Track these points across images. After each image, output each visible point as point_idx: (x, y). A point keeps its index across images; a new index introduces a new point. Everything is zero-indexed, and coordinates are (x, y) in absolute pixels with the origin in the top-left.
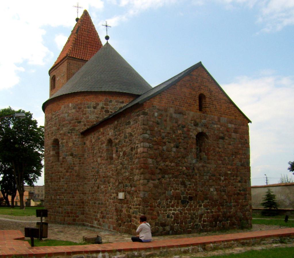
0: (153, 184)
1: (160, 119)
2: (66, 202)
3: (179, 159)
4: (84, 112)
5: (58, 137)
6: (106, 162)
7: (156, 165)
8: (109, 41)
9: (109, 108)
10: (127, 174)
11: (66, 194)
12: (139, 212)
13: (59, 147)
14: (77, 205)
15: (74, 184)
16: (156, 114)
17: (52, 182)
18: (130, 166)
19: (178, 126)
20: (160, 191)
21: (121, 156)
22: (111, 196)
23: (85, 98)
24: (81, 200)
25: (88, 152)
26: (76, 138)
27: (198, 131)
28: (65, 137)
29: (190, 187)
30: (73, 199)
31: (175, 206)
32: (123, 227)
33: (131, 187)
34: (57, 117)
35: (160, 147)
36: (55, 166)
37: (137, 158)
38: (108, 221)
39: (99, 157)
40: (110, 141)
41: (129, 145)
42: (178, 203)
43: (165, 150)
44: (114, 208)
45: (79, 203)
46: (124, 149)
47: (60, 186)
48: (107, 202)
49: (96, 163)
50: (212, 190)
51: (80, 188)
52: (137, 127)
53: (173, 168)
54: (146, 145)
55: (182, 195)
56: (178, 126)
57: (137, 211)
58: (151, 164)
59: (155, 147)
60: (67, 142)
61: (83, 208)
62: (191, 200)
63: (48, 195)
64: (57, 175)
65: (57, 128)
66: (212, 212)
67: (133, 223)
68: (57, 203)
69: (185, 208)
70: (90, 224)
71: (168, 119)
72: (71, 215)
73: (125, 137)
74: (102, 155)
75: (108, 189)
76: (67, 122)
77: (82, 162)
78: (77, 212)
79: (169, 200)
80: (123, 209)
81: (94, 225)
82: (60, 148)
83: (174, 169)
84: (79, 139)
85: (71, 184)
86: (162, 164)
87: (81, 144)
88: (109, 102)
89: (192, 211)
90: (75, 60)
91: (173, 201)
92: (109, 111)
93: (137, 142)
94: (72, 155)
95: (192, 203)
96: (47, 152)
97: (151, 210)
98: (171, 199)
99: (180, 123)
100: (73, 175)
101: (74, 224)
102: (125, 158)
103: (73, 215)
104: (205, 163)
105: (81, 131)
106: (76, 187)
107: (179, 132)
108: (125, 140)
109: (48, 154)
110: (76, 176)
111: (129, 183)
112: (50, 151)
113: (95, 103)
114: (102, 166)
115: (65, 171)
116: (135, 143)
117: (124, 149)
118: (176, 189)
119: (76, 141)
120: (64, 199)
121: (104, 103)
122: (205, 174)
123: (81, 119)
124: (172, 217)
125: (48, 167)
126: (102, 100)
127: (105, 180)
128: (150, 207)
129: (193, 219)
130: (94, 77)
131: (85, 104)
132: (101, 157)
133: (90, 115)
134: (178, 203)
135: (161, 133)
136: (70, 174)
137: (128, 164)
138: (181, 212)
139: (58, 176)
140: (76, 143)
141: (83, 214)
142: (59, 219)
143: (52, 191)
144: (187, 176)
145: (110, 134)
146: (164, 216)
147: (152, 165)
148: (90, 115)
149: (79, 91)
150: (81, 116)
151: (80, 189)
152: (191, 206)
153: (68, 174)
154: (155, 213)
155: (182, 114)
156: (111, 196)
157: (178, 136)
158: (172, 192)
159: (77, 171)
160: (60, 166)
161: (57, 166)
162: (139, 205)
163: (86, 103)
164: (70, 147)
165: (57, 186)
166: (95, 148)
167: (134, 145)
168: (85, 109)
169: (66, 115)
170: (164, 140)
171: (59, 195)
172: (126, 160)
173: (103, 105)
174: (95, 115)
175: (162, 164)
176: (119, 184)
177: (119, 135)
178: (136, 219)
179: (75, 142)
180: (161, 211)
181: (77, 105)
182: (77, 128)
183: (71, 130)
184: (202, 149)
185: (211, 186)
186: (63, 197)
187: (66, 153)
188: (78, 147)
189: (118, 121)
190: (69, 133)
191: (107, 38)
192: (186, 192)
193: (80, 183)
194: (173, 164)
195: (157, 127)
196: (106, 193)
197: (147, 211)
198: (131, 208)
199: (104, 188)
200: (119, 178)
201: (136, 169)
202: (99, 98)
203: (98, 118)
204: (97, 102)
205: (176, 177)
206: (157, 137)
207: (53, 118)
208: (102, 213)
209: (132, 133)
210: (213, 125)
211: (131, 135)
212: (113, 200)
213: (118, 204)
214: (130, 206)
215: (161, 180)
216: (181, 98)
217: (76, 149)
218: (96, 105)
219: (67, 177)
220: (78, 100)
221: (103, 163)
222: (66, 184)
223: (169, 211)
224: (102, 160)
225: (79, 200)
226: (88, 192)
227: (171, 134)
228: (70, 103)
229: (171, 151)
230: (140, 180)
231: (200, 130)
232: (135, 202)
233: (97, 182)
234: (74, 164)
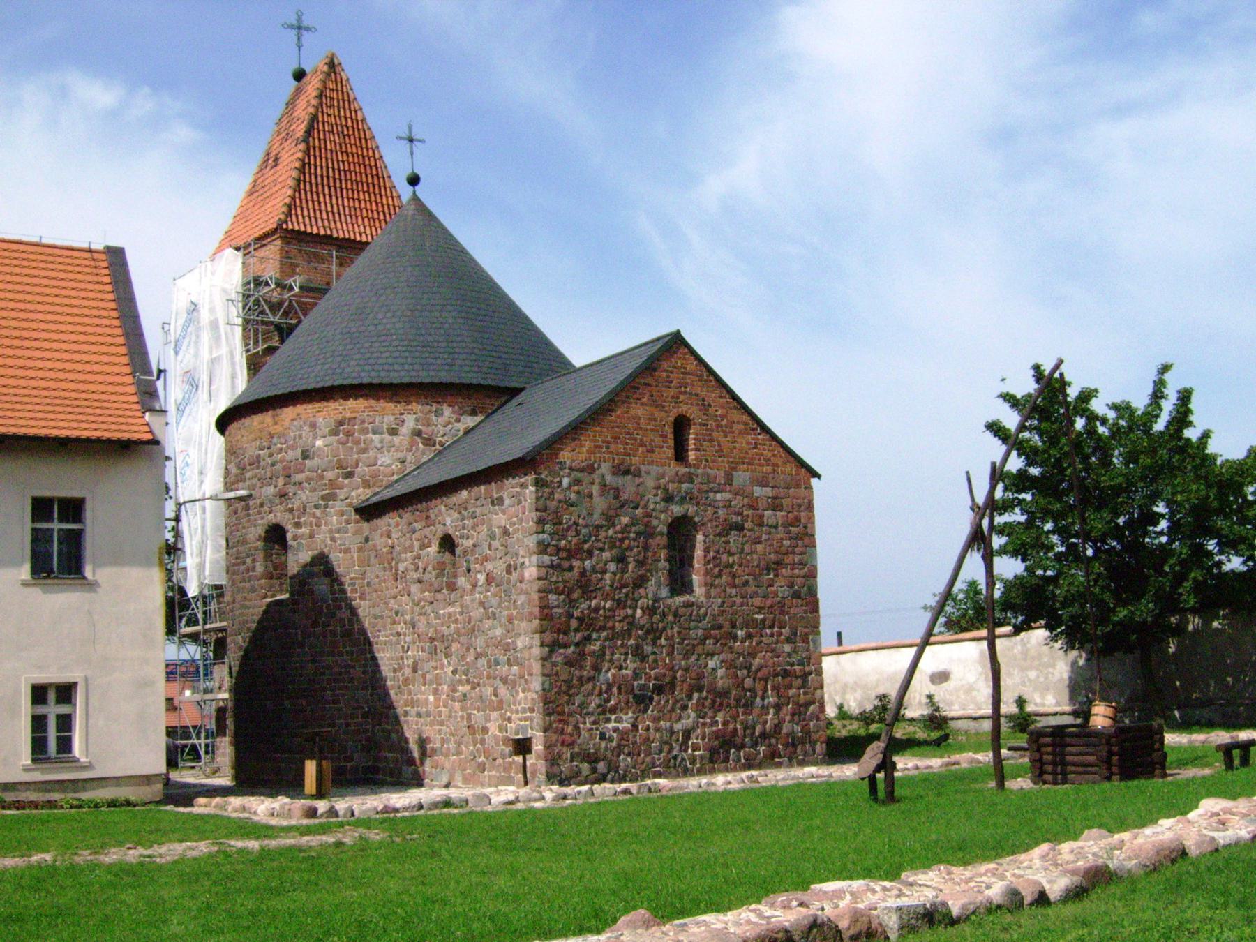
8: (419, 189)
12: (532, 729)
18: (505, 613)
29: (655, 661)
33: (510, 665)
35: (576, 563)
37: (522, 592)
46: (489, 566)
48: (443, 709)
71: (595, 489)
73: (492, 536)
93: (521, 552)
96: (244, 563)
99: (624, 497)
109: (248, 570)
111: (505, 655)
112: (254, 560)
116: (517, 554)
122: (693, 624)
131: (363, 422)
132: (420, 581)
133: (379, 456)
137: (499, 605)
146: (592, 737)
147: (560, 610)
154: (570, 729)
162: (532, 710)
172: (495, 595)
177: (473, 528)
181: (341, 423)
189: (470, 492)
190: (316, 507)
191: (414, 180)
195: (571, 514)
198: (509, 720)
201: (522, 620)
210: (711, 495)
214: (509, 714)
222: (314, 661)
229: (604, 572)
231: (677, 510)
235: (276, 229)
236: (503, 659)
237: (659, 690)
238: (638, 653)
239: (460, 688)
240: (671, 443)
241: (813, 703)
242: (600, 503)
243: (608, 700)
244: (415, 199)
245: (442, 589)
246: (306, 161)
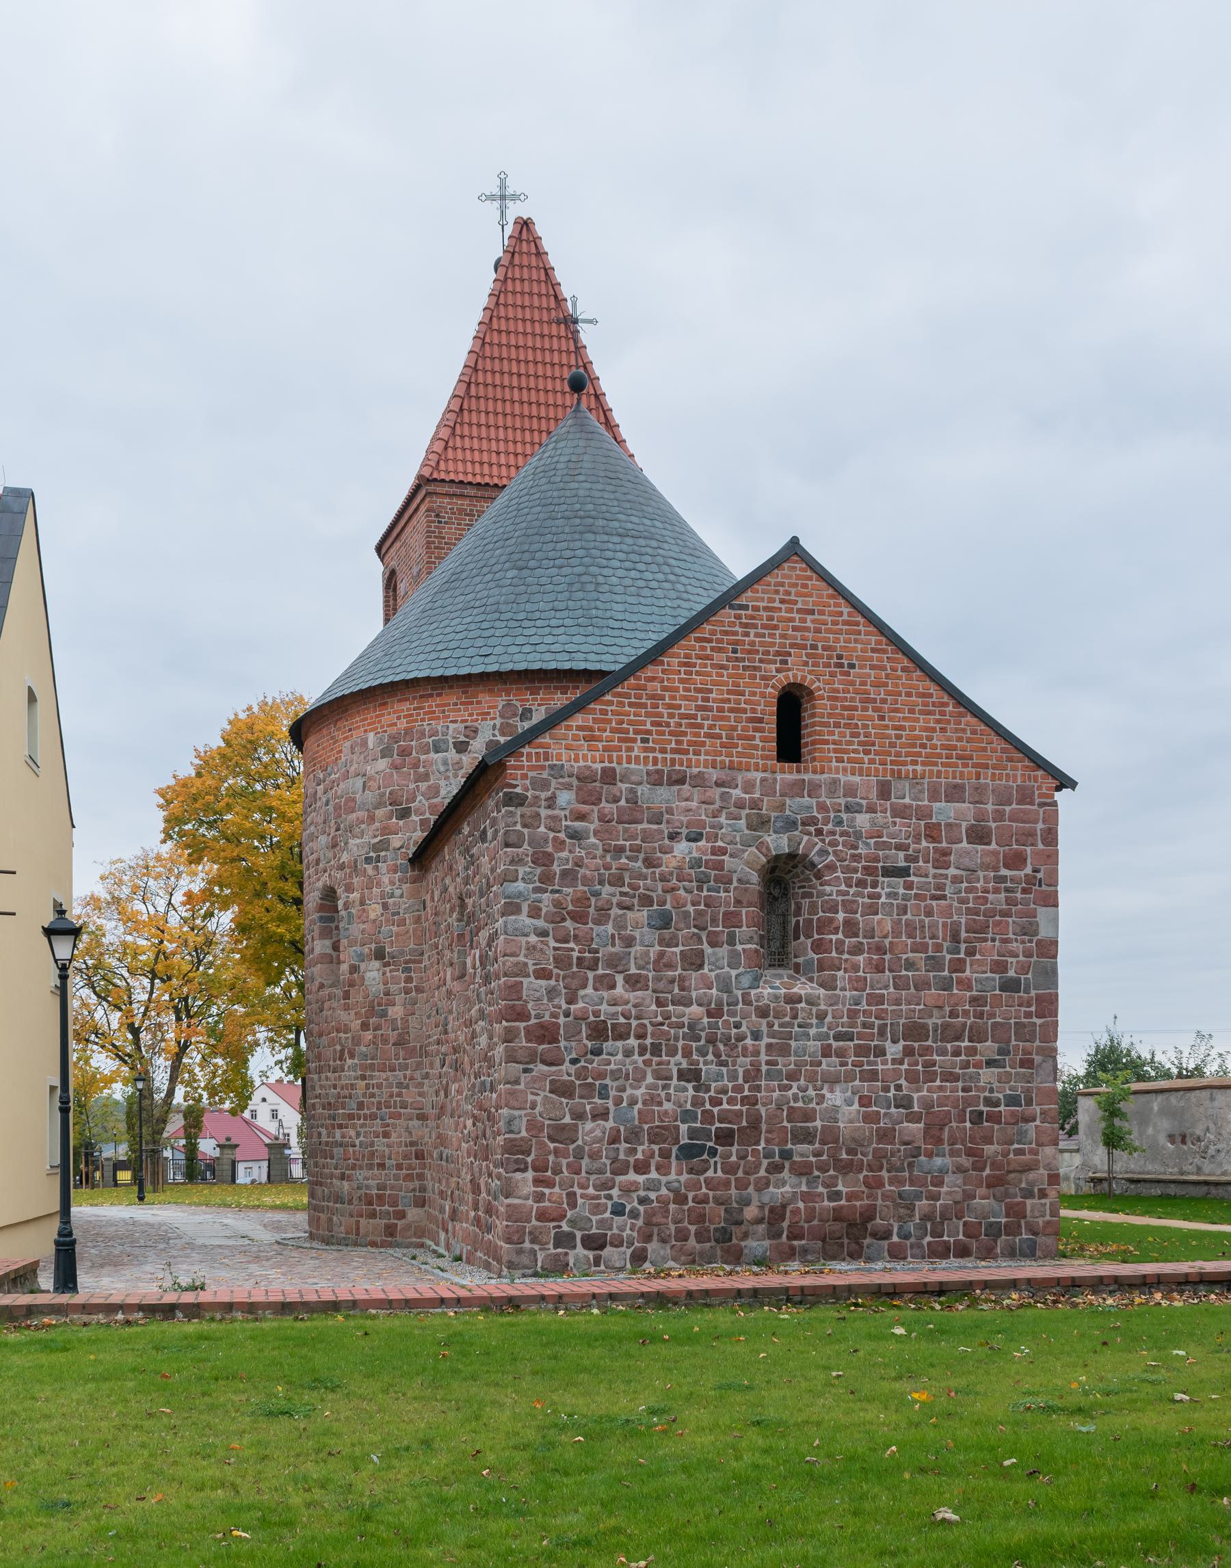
2: (363, 1156)
4: (421, 770)
11: (362, 1121)
15: (386, 1079)
17: (320, 1071)
23: (423, 708)
24: (412, 1144)
26: (392, 883)
28: (355, 880)
31: (653, 1168)
36: (327, 1005)
45: (406, 1157)
51: (410, 1096)
55: (683, 1122)
60: (362, 903)
61: (421, 1177)
66: (835, 1196)
76: (362, 814)
78: (402, 1194)
84: (405, 886)
85: (379, 1077)
90: (462, 496)
94: (379, 955)
95: (734, 1158)
100: (385, 1041)
101: (391, 1245)
103: (386, 1207)
106: (395, 1090)
115: (359, 1022)
119: (392, 896)
120: (357, 1143)
121: (498, 726)
123: (408, 801)
126: (488, 713)
128: (535, 1169)
131: (423, 734)
133: (442, 783)
134: (665, 1154)
136: (375, 1037)
138: (676, 1192)
139: (338, 1048)
140: (394, 904)
141: (421, 1203)
142: (342, 1229)
146: (597, 1209)
148: (442, 783)
149: (397, 678)
150: (412, 786)
151: (410, 1100)
152: (730, 1169)
153: (368, 1035)
159: (399, 1022)
161: (335, 1005)
164: (375, 921)
165: (335, 1087)
168: (423, 757)
169: (359, 782)
171: (340, 1126)
173: (494, 735)
179: (391, 901)
180: (583, 1186)
181: (395, 738)
182: (396, 841)
183: (375, 848)
185: (838, 1081)
187: (358, 949)
188: (402, 923)
190: (368, 860)
193: (408, 1073)
202: (478, 703)
204: (469, 724)
217: (395, 929)
218: (466, 736)
219: (364, 1049)
220: (399, 718)
222: (363, 1078)
225: (406, 1146)
228: (371, 730)
231: (779, 843)
234: (387, 994)
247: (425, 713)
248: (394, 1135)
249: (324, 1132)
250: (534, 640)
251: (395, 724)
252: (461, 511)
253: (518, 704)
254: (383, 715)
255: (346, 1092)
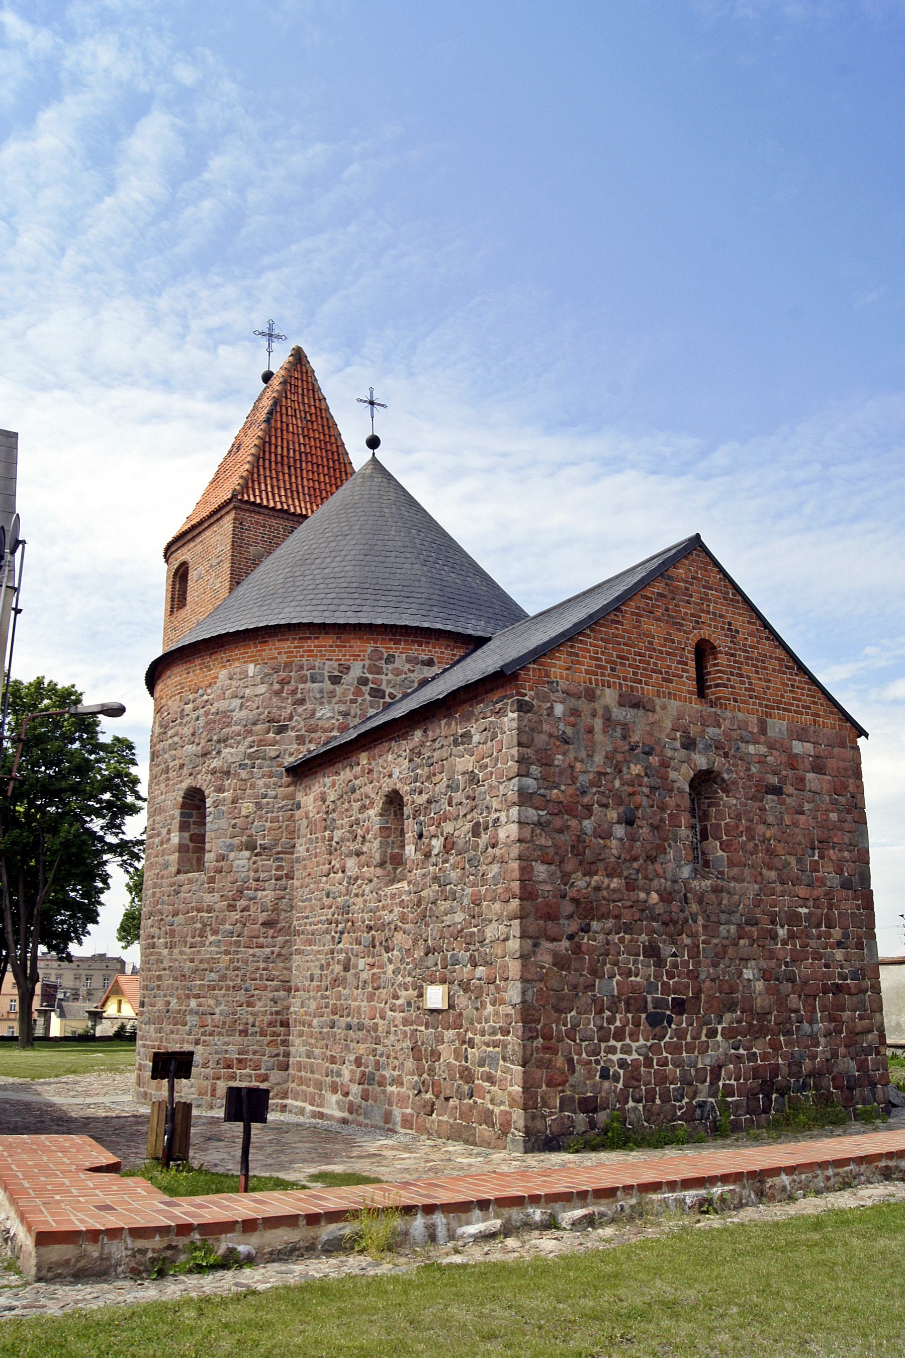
0: (556, 955)
1: (574, 725)
2: (224, 1023)
3: (636, 865)
5: (203, 781)
6: (379, 871)
7: (563, 887)
9: (384, 682)
10: (459, 917)
11: (223, 992)
13: (204, 816)
14: (263, 1034)
16: (559, 709)
17: (171, 946)
18: (469, 890)
19: (632, 749)
20: (572, 978)
21: (435, 852)
22: (396, 997)
23: (303, 647)
25: (309, 836)
27: (695, 764)
29: (675, 965)
30: (250, 1009)
32: (440, 1118)
33: (475, 966)
34: (202, 711)
35: (573, 823)
36: (186, 887)
38: (384, 1092)
39: (350, 855)
40: (394, 801)
41: (465, 815)
42: (637, 1024)
43: (589, 831)
44: (408, 1044)
45: (270, 1024)
46: (448, 827)
47: (201, 961)
48: (381, 1022)
49: (340, 874)
50: (748, 974)
52: (495, 754)
53: (616, 896)
54: (527, 817)
56: (632, 749)
57: (498, 1052)
58: (544, 882)
59: (558, 822)
60: (234, 802)
61: (285, 1043)
62: (681, 1013)
63: (155, 997)
64: (193, 920)
65: (199, 748)
67: (479, 1101)
68: (187, 1028)
69: (662, 1044)
70: (309, 1108)
71: (598, 724)
72: (238, 1072)
74: (365, 849)
75: (384, 973)
76: (236, 728)
77: (285, 872)
78: (266, 1058)
79: (608, 1013)
80: (440, 1048)
81: (325, 1111)
82: (208, 819)
83: (619, 901)
86: (581, 882)
87: (283, 806)
88: (383, 661)
89: (684, 1054)
91: (618, 1016)
92: (384, 692)
93: (495, 805)
94: (250, 846)
97: (546, 1049)
98: (614, 1008)
99: (635, 738)
102: (452, 860)
104: (723, 879)
105: (289, 761)
106: (262, 965)
107: (636, 769)
108: (451, 798)
109: (162, 843)
110: (264, 924)
113: (336, 664)
114: (364, 886)
117: (448, 827)
118: (630, 971)
119: (265, 796)
120: (217, 1011)
124: (616, 1079)
125: (158, 890)
126: (359, 656)
127: (374, 938)
129: (690, 1084)
130: (332, 575)
131: (301, 667)
132: (358, 854)
134: (637, 1024)
135: (575, 774)
137: (461, 880)
140: (268, 803)
143: (170, 981)
144: (665, 924)
145: (396, 772)
146: (590, 1074)
147: (549, 888)
149: (282, 622)
153: (236, 916)
154: (560, 1061)
155: (644, 708)
156: (396, 997)
157: (631, 784)
158: (614, 983)
160: (206, 886)
163: (305, 663)
164: (247, 817)
165: (192, 961)
166: (339, 822)
167: (484, 815)
168: (301, 686)
170: (586, 800)
171: (198, 996)
172: (454, 867)
174: (336, 706)
175: (581, 883)
176: (427, 954)
178: (493, 1083)
182: (272, 751)
183: (250, 756)
184: (709, 827)
186: (211, 1002)
187: (229, 841)
192: (663, 984)
194: (615, 883)
195: (564, 754)
196: (378, 988)
197: (535, 1055)
199: (367, 967)
200: (427, 930)
203: (346, 714)
204: (342, 662)
205: (628, 929)
206: (563, 787)
207: (188, 715)
208: (358, 1062)
209: (476, 771)
211: (473, 779)
212: (402, 1014)
213: (422, 1028)
214: (470, 1035)
215: (576, 939)
216: (640, 655)
217: (268, 824)
218: (341, 672)
220: (280, 653)
221: (367, 875)
222: (227, 953)
223: (607, 1052)
224: (363, 867)
225: (272, 1014)
226: (307, 983)
227: (608, 777)
228: (251, 662)
230: (507, 939)
232: (487, 1021)
233: (341, 946)
235: (231, 500)
236: (464, 956)
237: (680, 1006)
238: (652, 952)
239: (403, 993)
240: (693, 673)
241: (870, 1031)
242: (603, 742)
243: (611, 1021)
244: (374, 460)
245: (385, 862)
246: (267, 440)
247: (304, 652)
248: (259, 1004)
249: (174, 1001)
250: (392, 604)
251: (276, 658)
252: (257, 523)
253: (384, 650)
254: (265, 650)
255: (205, 966)
